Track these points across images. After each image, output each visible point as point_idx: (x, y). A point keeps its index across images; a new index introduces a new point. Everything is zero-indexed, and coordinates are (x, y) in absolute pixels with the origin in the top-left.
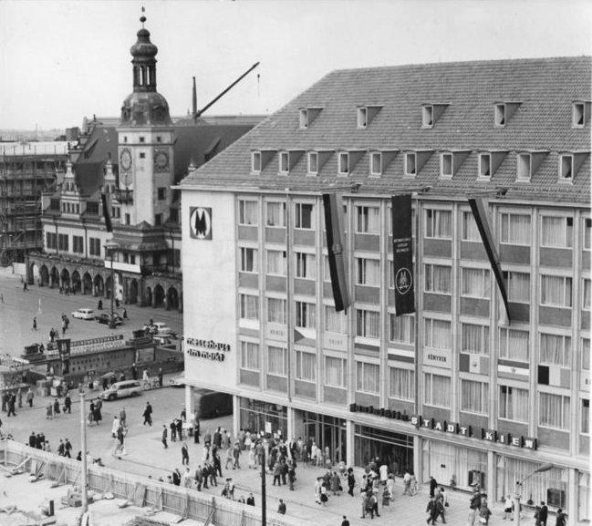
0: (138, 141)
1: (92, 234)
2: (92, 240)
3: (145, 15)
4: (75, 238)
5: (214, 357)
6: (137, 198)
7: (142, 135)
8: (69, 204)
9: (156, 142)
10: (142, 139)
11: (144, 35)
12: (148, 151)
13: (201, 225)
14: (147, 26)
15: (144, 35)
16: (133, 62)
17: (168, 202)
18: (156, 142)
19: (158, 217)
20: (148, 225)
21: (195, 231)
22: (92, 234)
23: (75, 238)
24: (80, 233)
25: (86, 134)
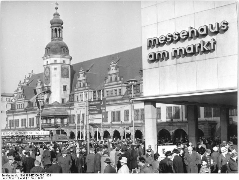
0: (53, 62)
3: (57, 6)
5: (194, 52)
6: (52, 89)
7: (55, 59)
8: (19, 105)
9: (63, 63)
10: (55, 61)
12: (59, 67)
14: (58, 11)
15: (57, 15)
16: (51, 27)
17: (68, 92)
18: (63, 63)
19: (63, 100)
20: (58, 103)
22: (31, 116)
23: (22, 120)
24: (24, 117)
25: (28, 78)
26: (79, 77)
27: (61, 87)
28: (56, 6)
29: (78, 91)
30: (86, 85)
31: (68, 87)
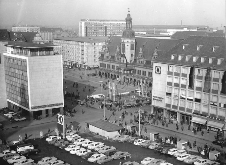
0: (127, 42)
1: (112, 64)
2: (112, 66)
4: (108, 65)
5: (159, 100)
7: (128, 40)
10: (128, 41)
11: (129, 15)
12: (129, 45)
13: (158, 70)
14: (130, 13)
15: (129, 15)
21: (156, 72)
22: (112, 64)
23: (108, 65)
24: (109, 63)
26: (139, 52)
27: (130, 55)
28: (128, 10)
29: (139, 58)
30: (143, 57)
31: (134, 54)
